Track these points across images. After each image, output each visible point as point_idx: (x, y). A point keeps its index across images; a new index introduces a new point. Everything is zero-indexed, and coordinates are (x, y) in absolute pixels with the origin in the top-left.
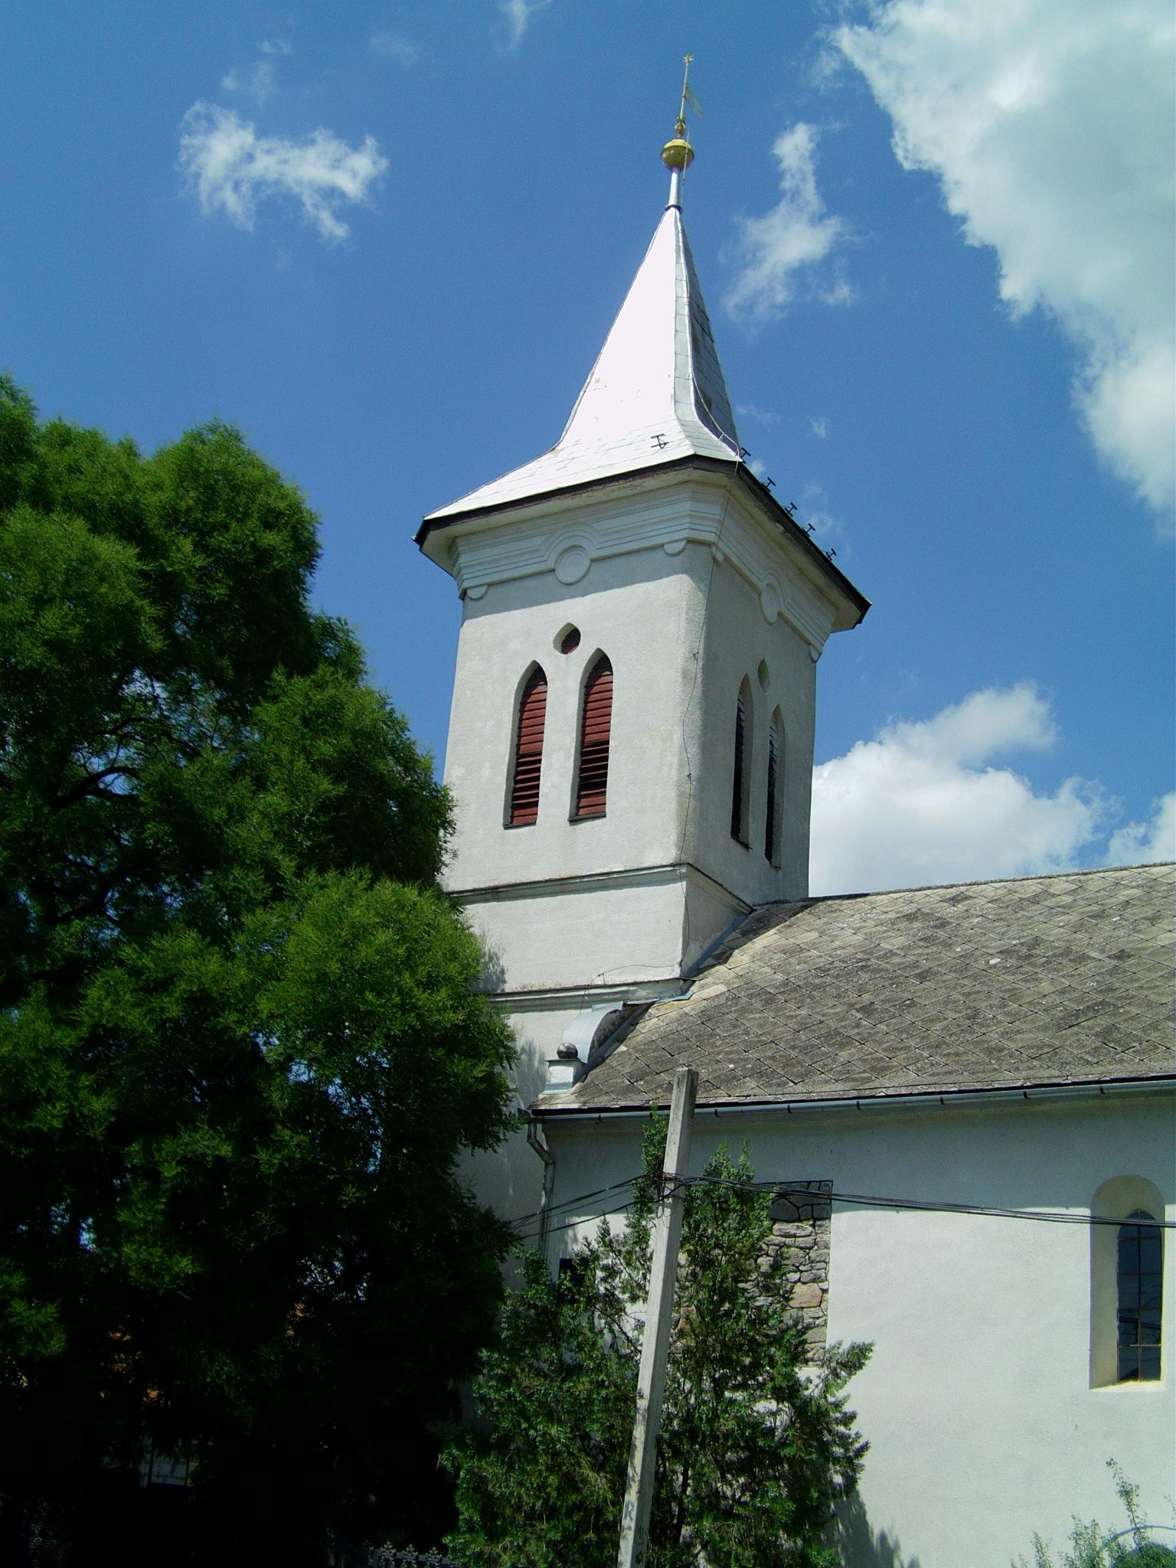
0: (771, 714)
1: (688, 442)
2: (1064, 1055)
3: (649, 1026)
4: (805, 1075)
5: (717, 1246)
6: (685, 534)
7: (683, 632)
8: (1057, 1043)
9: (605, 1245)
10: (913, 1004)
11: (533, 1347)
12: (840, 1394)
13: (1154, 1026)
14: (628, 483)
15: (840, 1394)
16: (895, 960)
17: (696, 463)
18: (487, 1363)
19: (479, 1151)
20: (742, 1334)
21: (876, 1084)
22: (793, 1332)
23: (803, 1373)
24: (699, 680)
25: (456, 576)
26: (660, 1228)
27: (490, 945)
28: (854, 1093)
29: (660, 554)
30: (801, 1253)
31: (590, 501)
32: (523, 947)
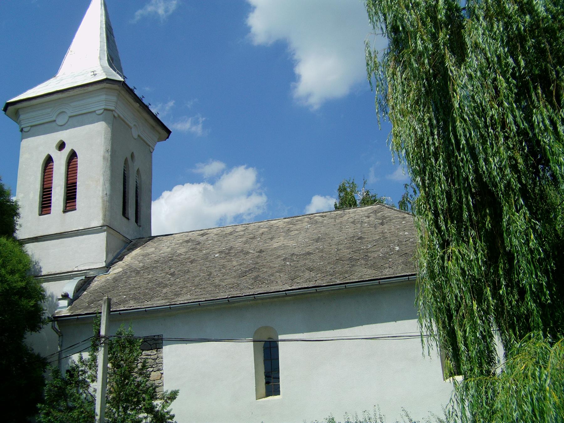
0: (136, 172)
1: (104, 74)
2: (242, 286)
3: (95, 285)
4: (151, 299)
5: (122, 360)
6: (103, 107)
7: (103, 142)
8: (239, 282)
9: (81, 362)
10: (189, 271)
11: (57, 401)
12: (168, 409)
13: (272, 275)
14: (86, 88)
15: (168, 409)
16: (182, 257)
17: (107, 81)
18: (40, 409)
19: (33, 333)
20: (133, 390)
21: (176, 300)
22: (151, 388)
23: (155, 403)
24: (109, 159)
25: (19, 123)
26: (100, 355)
27: (35, 258)
28: (169, 304)
29: (94, 114)
30: (153, 361)
31: (69, 95)
32: (48, 258)
